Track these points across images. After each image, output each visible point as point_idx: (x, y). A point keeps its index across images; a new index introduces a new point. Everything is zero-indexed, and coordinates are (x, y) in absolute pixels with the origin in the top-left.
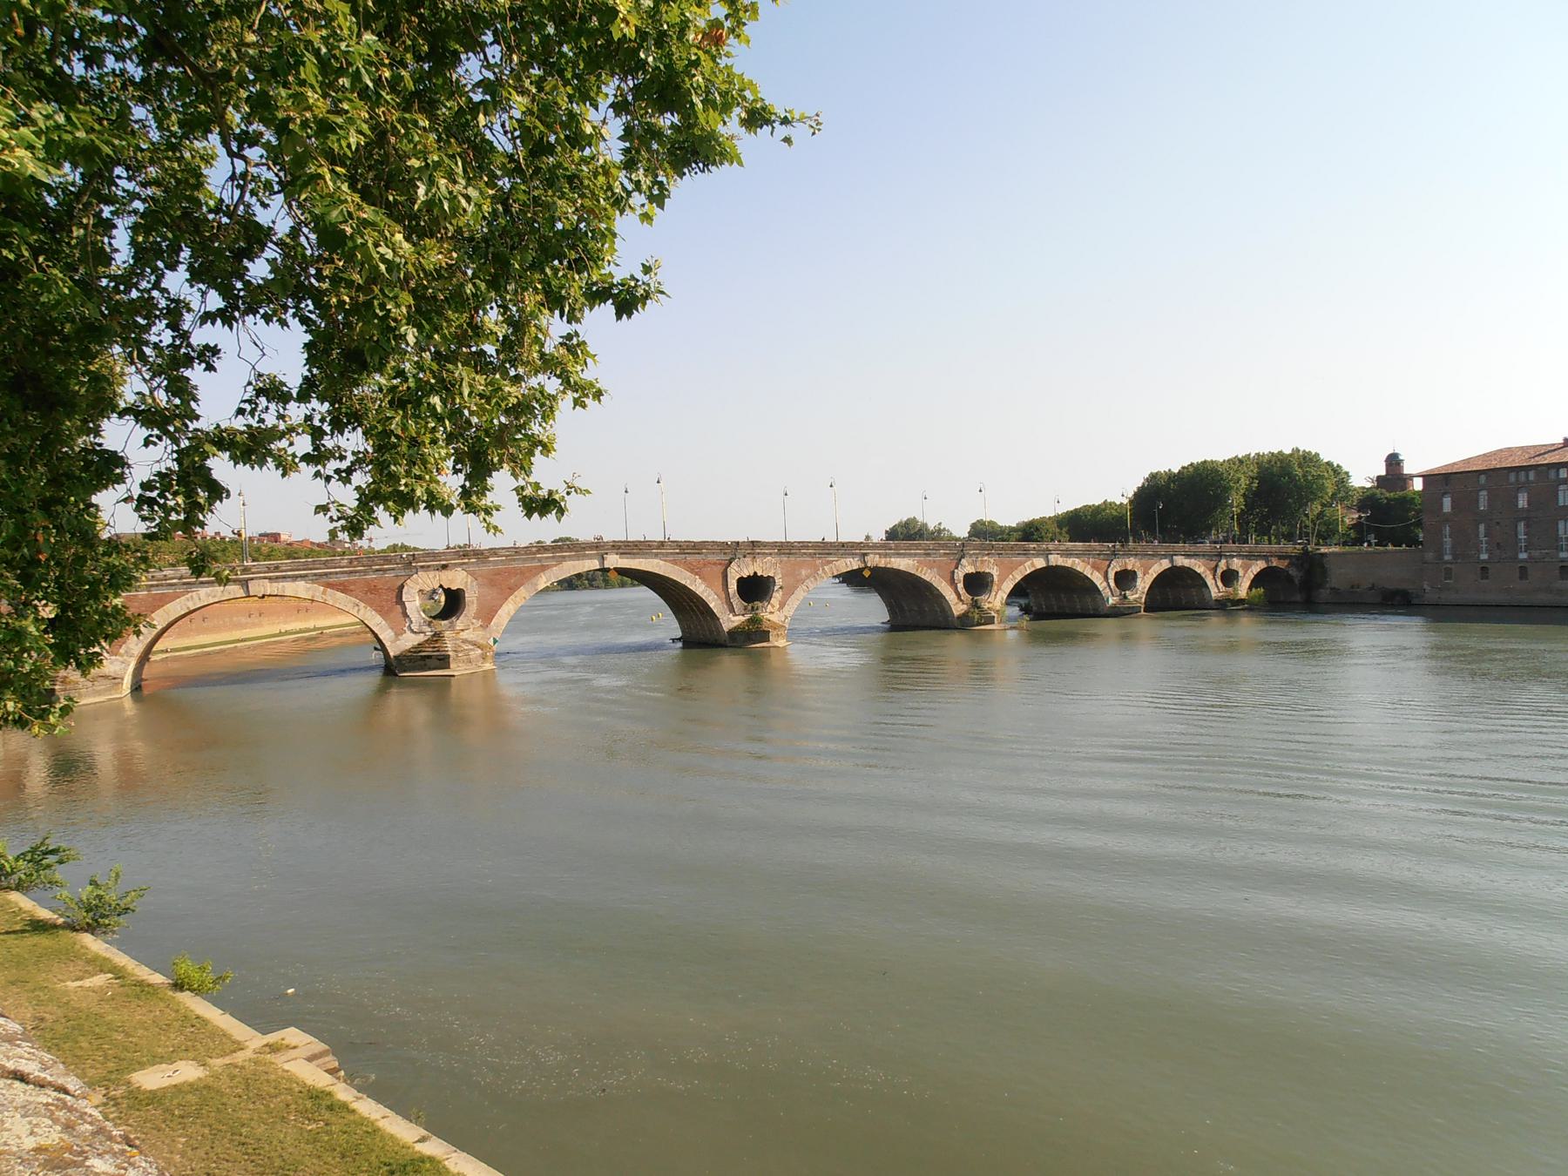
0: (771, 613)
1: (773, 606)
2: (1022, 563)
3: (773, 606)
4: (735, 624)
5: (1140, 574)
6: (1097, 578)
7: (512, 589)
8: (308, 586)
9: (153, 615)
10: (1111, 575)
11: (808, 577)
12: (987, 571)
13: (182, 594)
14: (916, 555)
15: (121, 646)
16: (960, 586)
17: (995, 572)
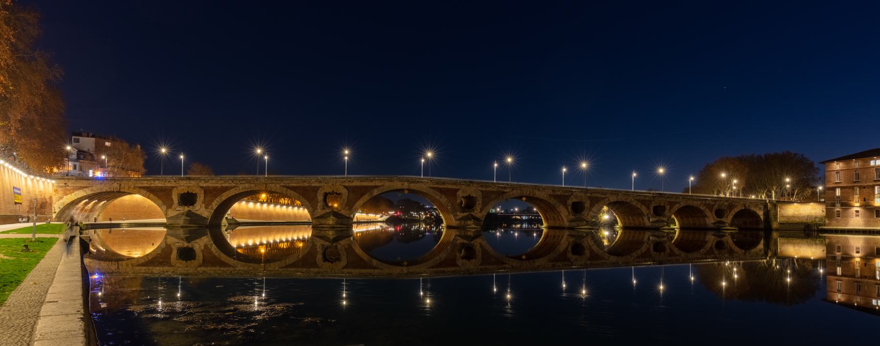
0: (476, 213)
1: (477, 211)
3: (477, 211)
4: (460, 217)
5: (668, 207)
6: (644, 209)
7: (363, 195)
8: (281, 187)
9: (222, 195)
10: (652, 208)
13: (234, 187)
15: (209, 206)
16: (570, 208)
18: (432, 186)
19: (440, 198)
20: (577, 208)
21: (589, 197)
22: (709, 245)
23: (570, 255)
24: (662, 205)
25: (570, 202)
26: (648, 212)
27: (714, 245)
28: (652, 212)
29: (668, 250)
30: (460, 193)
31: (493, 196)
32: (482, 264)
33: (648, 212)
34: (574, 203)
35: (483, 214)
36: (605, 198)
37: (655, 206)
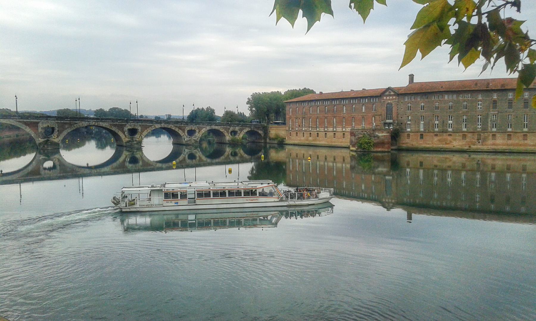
0: (54, 139)
1: (55, 136)
2: (151, 126)
4: (41, 142)
5: (197, 131)
6: (180, 132)
10: (186, 131)
11: (68, 128)
12: (137, 128)
14: (109, 122)
17: (139, 129)
18: (18, 120)
19: (25, 128)
20: (133, 132)
21: (140, 125)
22: (226, 154)
23: (127, 164)
24: (193, 129)
25: (126, 129)
26: (183, 134)
27: (230, 153)
28: (186, 134)
29: (198, 158)
30: (40, 125)
31: (66, 126)
32: (60, 173)
33: (183, 134)
34: (129, 130)
35: (60, 139)
36: (152, 126)
37: (188, 130)
